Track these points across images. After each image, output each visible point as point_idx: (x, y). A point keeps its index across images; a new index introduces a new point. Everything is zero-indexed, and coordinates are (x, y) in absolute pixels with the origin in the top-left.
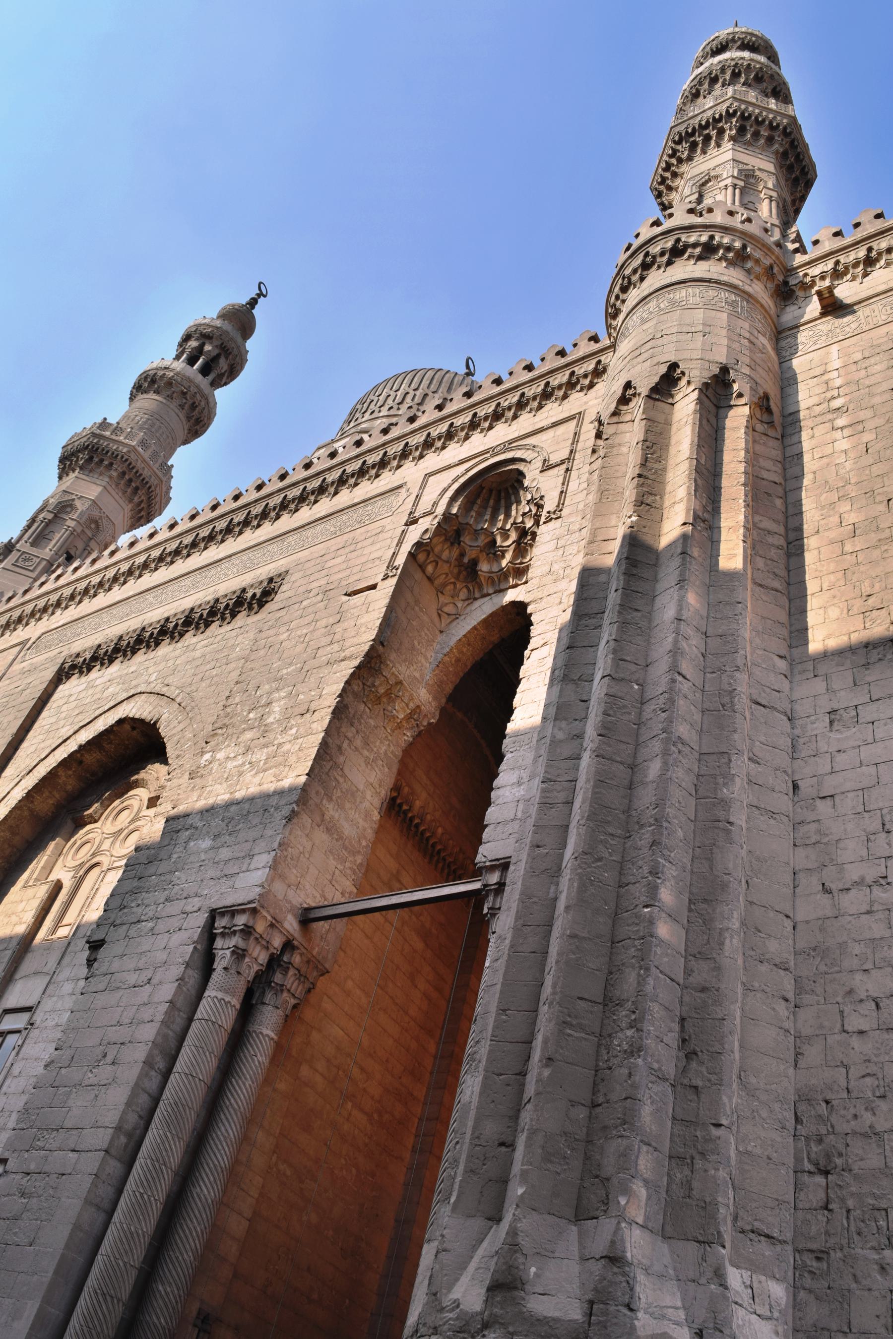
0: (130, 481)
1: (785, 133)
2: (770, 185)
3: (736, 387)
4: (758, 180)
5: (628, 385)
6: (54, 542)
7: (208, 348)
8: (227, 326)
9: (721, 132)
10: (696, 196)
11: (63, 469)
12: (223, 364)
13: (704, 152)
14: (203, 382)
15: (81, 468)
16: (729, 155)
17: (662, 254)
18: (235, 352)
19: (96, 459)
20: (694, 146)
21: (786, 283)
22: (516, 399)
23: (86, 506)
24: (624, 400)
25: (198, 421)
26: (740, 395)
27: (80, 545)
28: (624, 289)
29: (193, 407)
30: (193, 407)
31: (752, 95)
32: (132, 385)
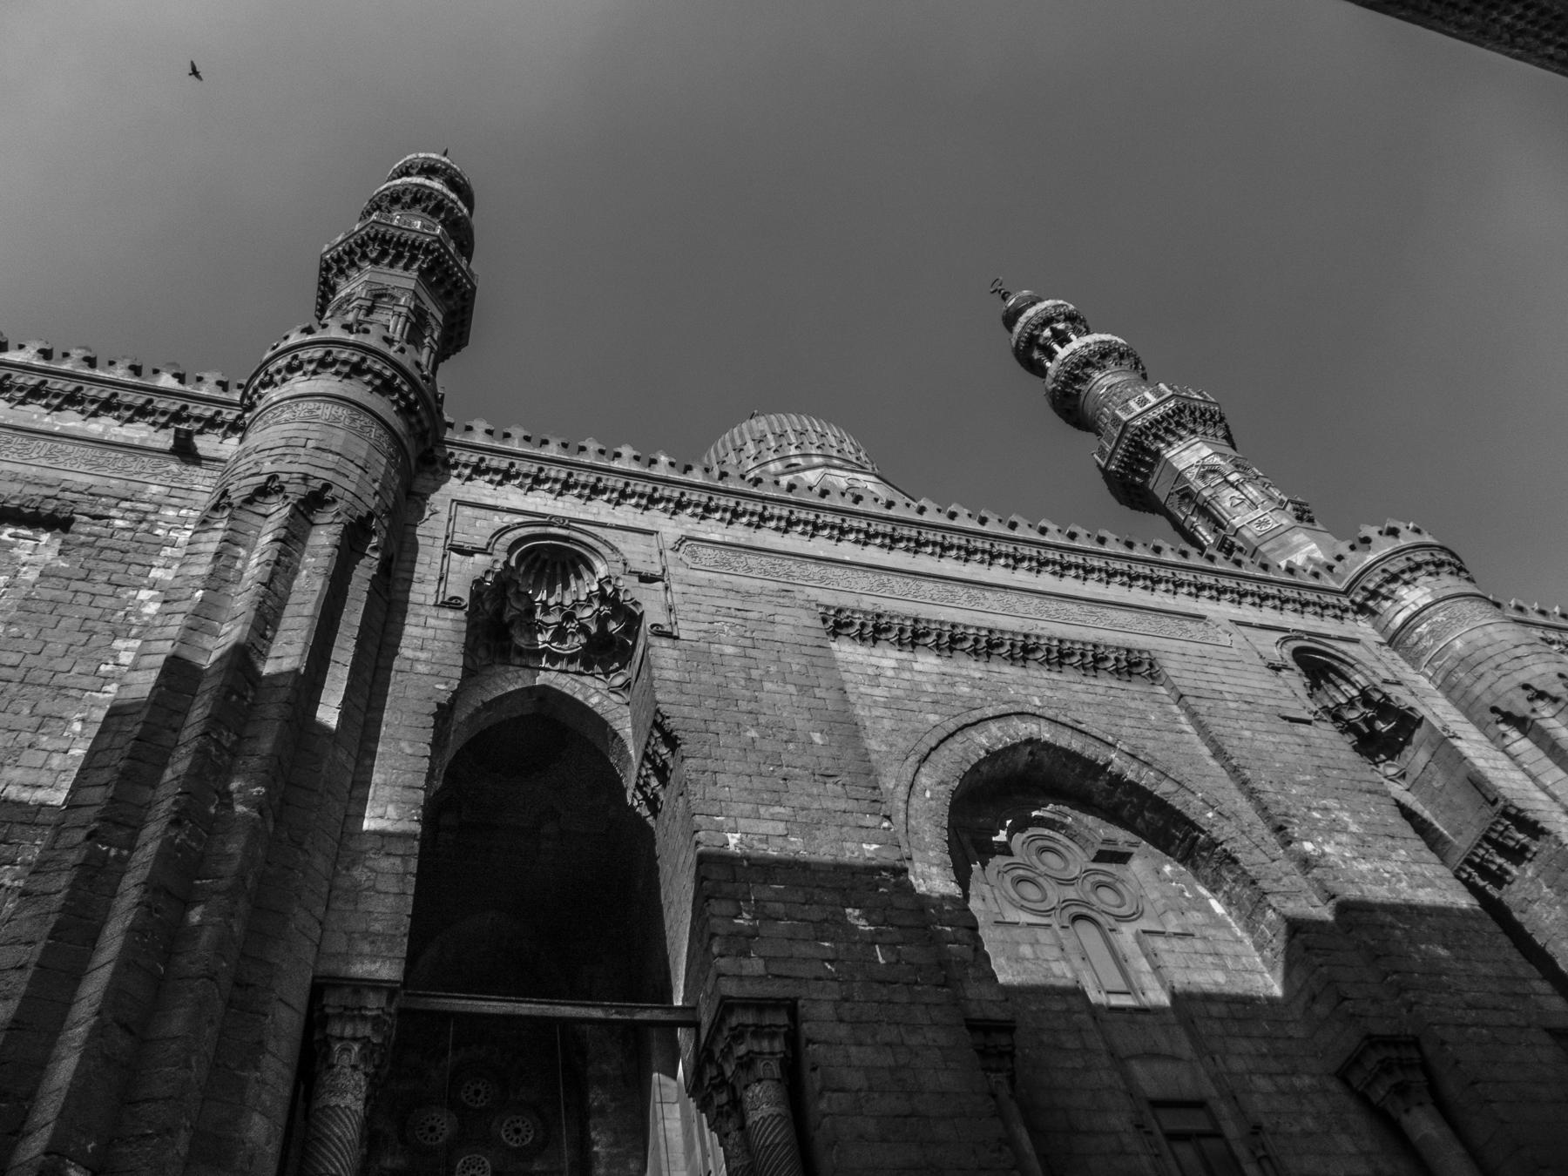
1: (463, 297)
2: (436, 336)
3: (375, 540)
4: (426, 324)
5: (273, 477)
9: (413, 259)
10: (369, 303)
13: (391, 265)
16: (412, 285)
17: (345, 362)
20: (383, 254)
21: (432, 451)
22: (105, 395)
24: (263, 492)
26: (375, 549)
28: (291, 369)
31: (452, 247)
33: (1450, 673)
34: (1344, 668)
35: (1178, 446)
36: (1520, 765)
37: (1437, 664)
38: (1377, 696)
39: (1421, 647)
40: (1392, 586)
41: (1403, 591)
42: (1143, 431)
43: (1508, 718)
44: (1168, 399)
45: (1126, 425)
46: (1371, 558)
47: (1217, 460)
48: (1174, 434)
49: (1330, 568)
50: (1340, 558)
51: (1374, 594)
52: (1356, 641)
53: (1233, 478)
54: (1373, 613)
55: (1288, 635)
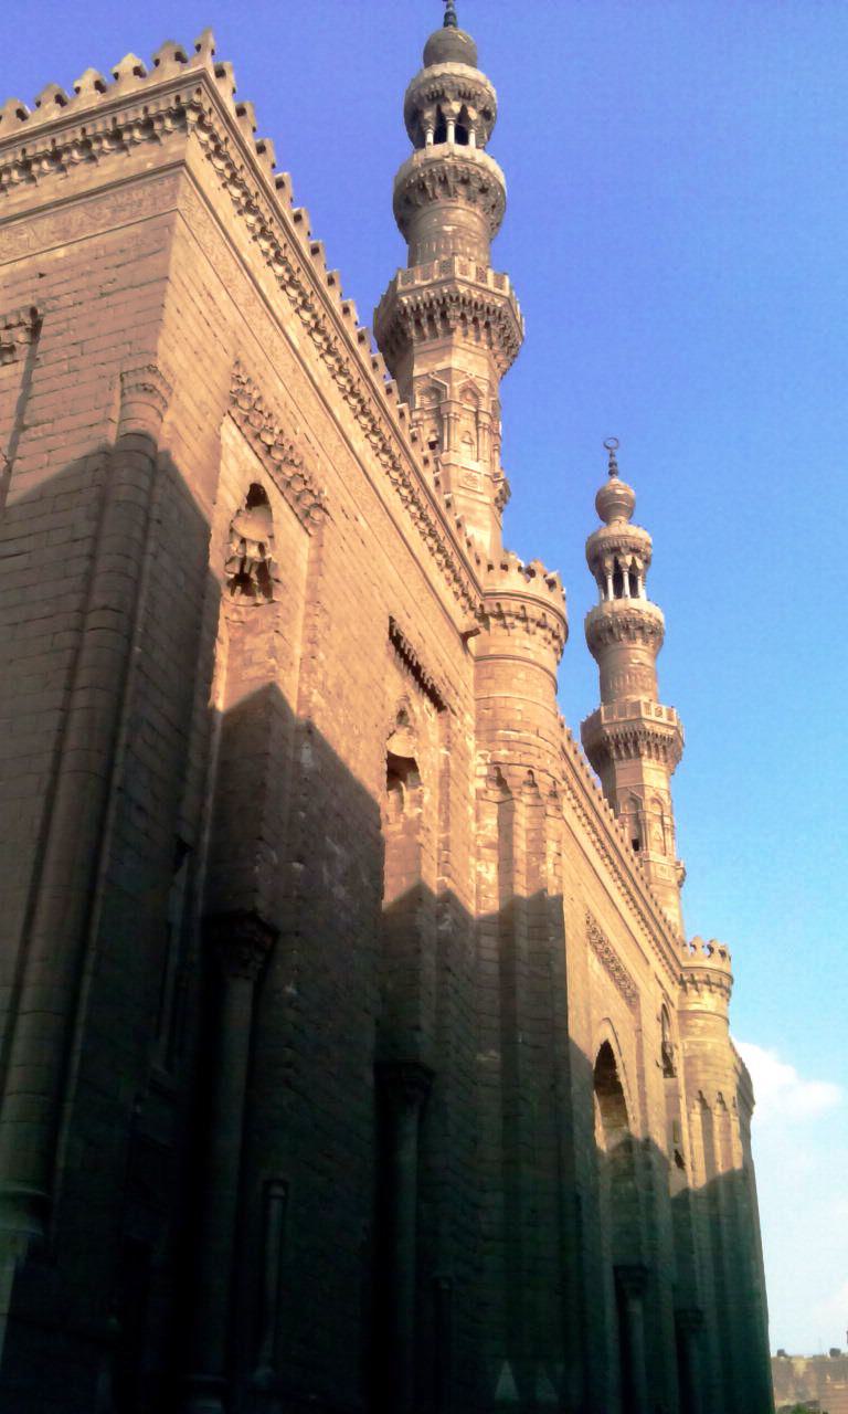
33: (695, 1056)
34: (667, 1025)
35: (654, 760)
36: (690, 1126)
37: (694, 1047)
38: (668, 1051)
39: (694, 1030)
40: (705, 987)
41: (706, 994)
42: (647, 734)
43: (703, 1101)
44: (672, 727)
45: (640, 719)
46: (708, 963)
47: (665, 797)
48: (657, 751)
49: (685, 945)
50: (694, 946)
51: (694, 982)
52: (673, 1005)
53: (667, 820)
54: (685, 990)
55: (666, 996)
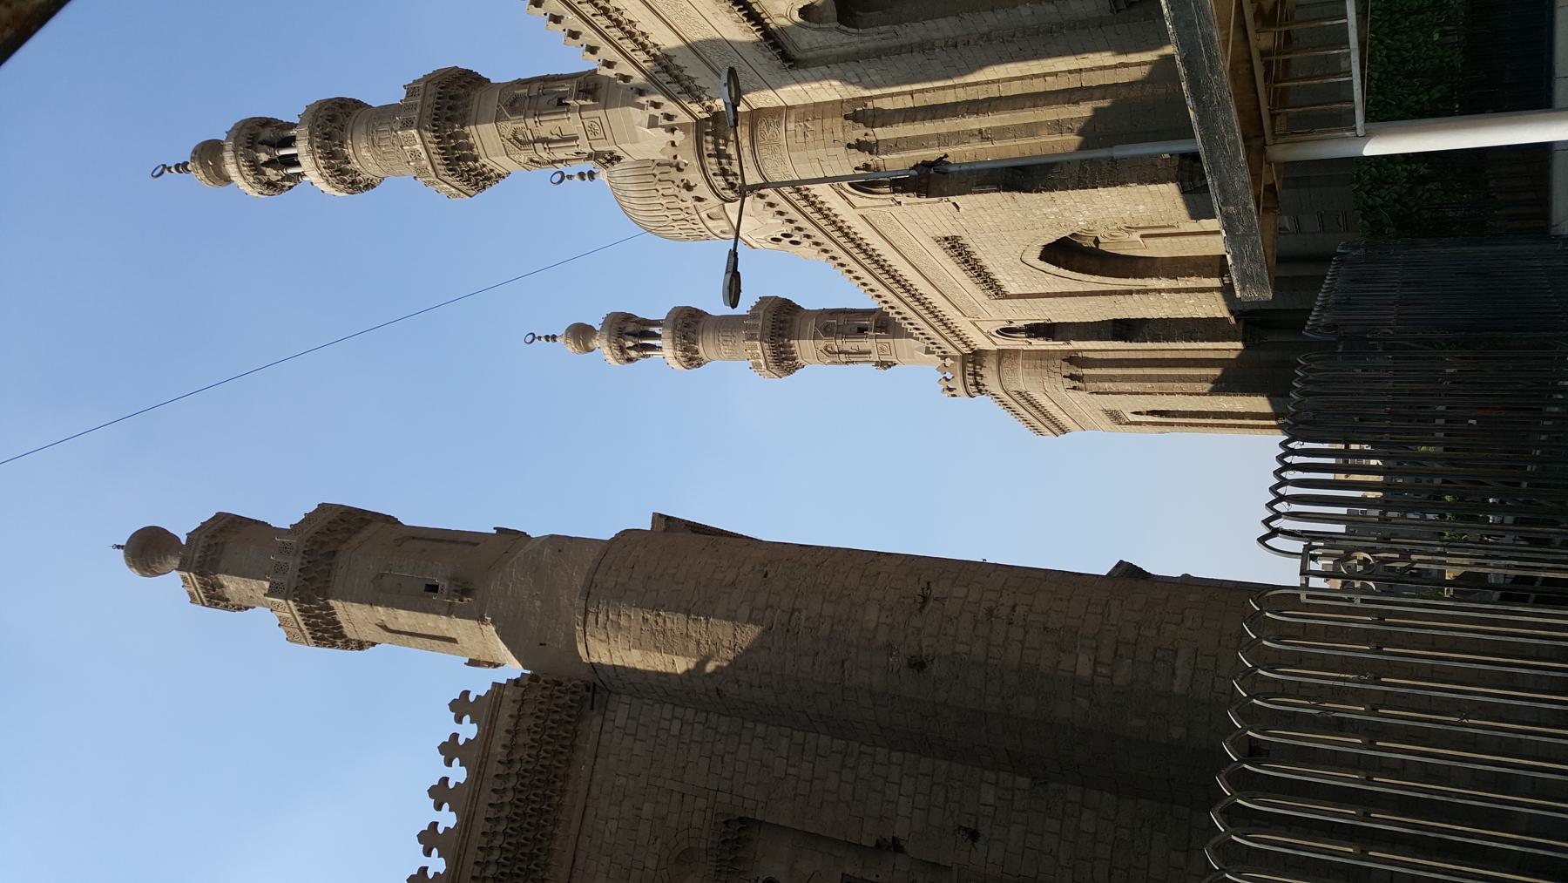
0: (450, 108)
6: (559, 123)
7: (264, 157)
8: (228, 156)
11: (490, 178)
12: (267, 134)
14: (301, 134)
15: (476, 160)
18: (245, 131)
19: (457, 153)
23: (502, 124)
25: (341, 106)
27: (543, 101)
29: (332, 119)
30: (332, 119)
32: (358, 196)
